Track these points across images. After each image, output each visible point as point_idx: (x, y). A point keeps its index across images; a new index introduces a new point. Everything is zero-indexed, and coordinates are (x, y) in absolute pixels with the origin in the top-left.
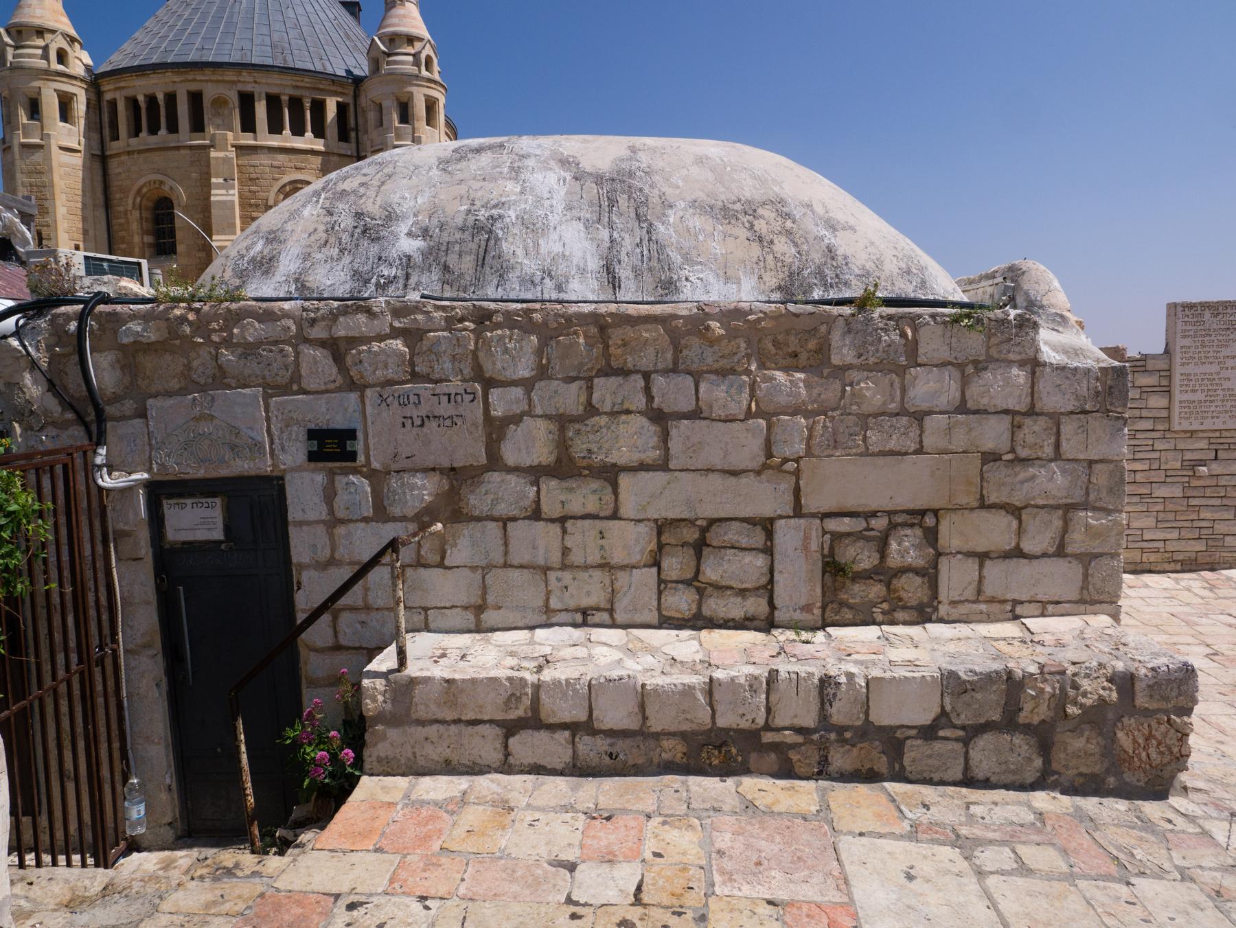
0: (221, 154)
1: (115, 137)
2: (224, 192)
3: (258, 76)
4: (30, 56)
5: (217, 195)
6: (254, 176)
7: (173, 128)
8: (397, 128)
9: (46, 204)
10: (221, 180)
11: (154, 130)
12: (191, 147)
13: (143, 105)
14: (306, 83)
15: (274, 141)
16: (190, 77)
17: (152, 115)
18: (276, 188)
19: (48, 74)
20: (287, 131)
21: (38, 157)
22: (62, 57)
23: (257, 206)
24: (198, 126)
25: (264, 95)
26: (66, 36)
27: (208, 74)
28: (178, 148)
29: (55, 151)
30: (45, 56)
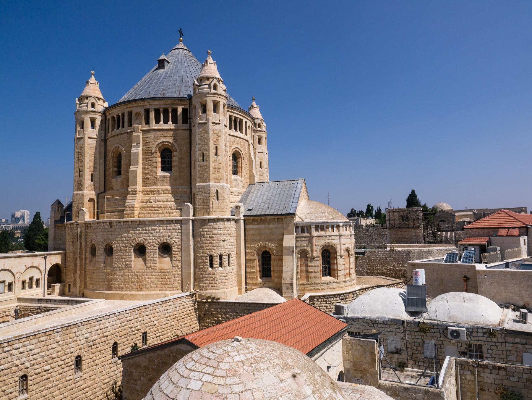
0: (136, 134)
1: (109, 132)
2: (135, 149)
3: (151, 102)
4: (83, 106)
5: (134, 150)
6: (148, 141)
7: (123, 127)
8: (200, 116)
9: (82, 159)
10: (135, 144)
11: (118, 128)
12: (128, 133)
13: (116, 119)
14: (170, 102)
15: (156, 127)
16: (128, 106)
17: (119, 122)
18: (155, 146)
19: (87, 112)
20: (162, 122)
21: (81, 142)
22: (93, 105)
23: (148, 153)
24: (130, 125)
25: (153, 109)
26: (95, 97)
27: (134, 104)
28: (124, 134)
29: (87, 138)
30: (87, 106)
